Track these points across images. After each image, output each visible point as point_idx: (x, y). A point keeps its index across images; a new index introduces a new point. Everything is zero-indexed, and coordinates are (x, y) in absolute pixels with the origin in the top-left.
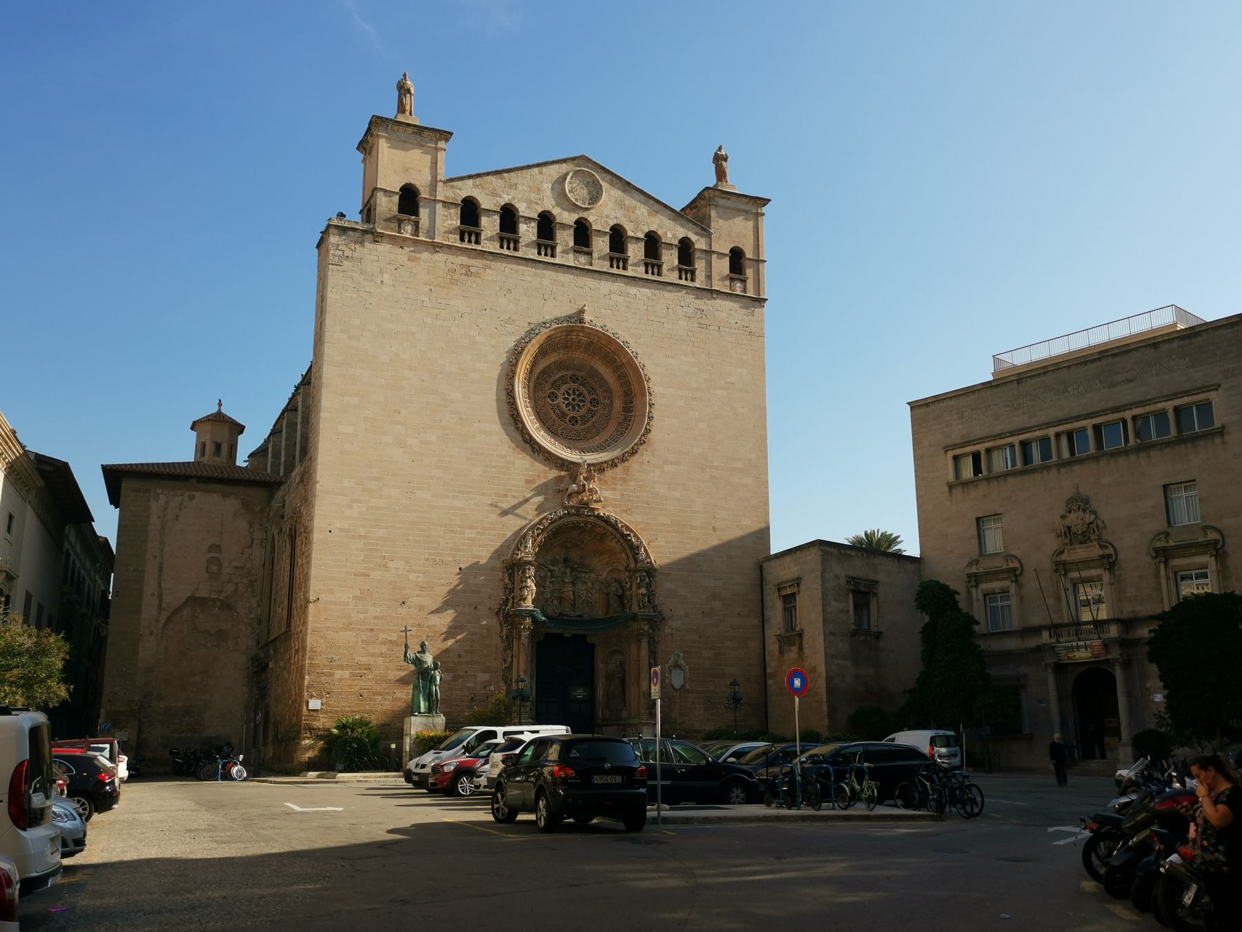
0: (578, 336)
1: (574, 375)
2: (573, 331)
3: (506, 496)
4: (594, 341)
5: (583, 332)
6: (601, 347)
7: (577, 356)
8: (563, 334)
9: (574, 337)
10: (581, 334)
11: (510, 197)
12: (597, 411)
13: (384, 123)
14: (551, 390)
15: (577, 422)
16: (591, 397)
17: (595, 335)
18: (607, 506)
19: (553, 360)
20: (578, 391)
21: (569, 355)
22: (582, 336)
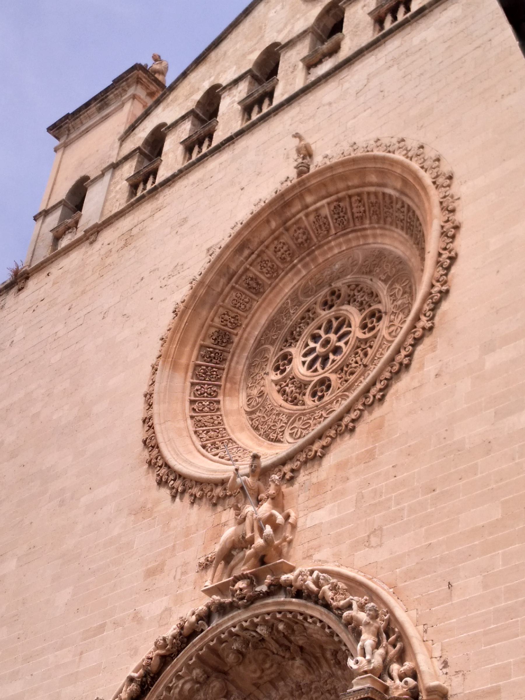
0: (307, 207)
1: (333, 293)
2: (288, 204)
3: (102, 628)
4: (340, 195)
5: (309, 191)
6: (359, 195)
7: (336, 251)
8: (273, 224)
9: (301, 215)
10: (309, 199)
11: (212, 78)
12: (375, 336)
13: (62, 129)
14: (282, 352)
15: (329, 387)
16: (363, 315)
17: (333, 179)
18: (319, 548)
19: (287, 290)
20: (337, 318)
21: (321, 260)
22: (315, 203)
